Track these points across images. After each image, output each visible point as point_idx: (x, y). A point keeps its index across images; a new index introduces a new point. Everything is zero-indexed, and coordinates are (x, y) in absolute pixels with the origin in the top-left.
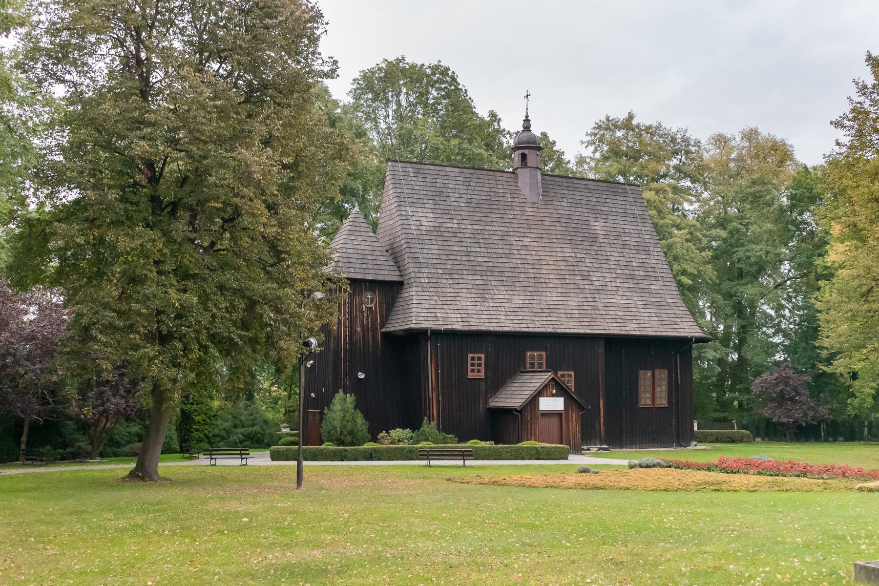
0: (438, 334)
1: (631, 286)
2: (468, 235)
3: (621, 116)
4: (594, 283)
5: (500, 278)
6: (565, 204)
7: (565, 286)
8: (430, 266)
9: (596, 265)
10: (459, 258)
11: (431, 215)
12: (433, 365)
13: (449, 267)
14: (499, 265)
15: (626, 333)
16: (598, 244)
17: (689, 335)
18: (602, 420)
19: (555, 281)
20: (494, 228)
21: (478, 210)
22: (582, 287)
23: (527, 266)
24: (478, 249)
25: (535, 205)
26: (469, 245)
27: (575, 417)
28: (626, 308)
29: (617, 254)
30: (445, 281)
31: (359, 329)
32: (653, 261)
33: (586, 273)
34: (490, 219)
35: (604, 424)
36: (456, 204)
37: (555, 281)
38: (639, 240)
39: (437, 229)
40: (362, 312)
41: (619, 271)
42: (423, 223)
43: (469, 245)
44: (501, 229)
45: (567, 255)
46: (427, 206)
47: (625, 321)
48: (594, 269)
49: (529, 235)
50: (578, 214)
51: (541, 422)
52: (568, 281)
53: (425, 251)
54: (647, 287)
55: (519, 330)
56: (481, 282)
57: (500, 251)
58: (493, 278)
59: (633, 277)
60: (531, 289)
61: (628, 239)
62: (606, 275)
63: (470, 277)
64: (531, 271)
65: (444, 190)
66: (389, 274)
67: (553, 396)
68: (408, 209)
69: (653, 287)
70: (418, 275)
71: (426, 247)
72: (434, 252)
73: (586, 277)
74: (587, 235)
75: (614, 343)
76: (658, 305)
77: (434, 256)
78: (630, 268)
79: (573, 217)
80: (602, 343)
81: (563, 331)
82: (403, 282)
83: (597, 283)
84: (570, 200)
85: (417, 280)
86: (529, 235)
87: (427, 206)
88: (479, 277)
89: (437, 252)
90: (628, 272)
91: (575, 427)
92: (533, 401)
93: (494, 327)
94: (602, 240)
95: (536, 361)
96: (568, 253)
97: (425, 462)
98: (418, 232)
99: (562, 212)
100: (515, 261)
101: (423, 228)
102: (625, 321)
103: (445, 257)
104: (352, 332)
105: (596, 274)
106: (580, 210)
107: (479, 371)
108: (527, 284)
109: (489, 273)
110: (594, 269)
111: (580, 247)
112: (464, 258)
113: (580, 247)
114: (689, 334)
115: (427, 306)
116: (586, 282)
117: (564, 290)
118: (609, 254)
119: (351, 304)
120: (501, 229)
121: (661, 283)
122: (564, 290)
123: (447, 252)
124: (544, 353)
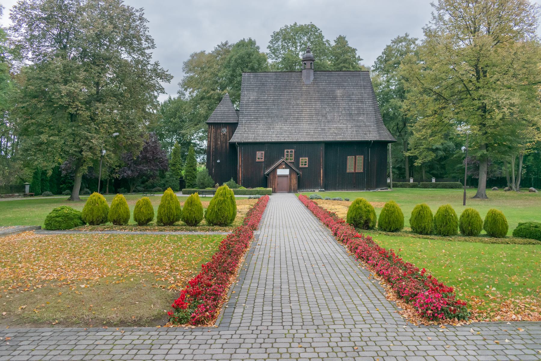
0: (239, 144)
1: (348, 118)
2: (270, 101)
3: (402, 35)
4: (328, 118)
5: (280, 119)
6: (324, 84)
7: (312, 120)
8: (249, 115)
9: (331, 110)
10: (263, 111)
11: (256, 94)
13: (257, 115)
14: (282, 113)
15: (335, 140)
16: (336, 100)
17: (369, 140)
19: (307, 118)
20: (284, 97)
21: (279, 90)
22: (321, 120)
23: (295, 113)
24: (273, 107)
25: (308, 85)
26: (270, 105)
27: (294, 177)
28: (341, 129)
29: (345, 104)
30: (254, 121)
32: (364, 106)
33: (325, 114)
34: (283, 93)
35: (322, 180)
36: (269, 88)
37: (307, 118)
38: (360, 97)
41: (343, 112)
42: (251, 98)
43: (270, 105)
44: (288, 97)
45: (317, 106)
46: (255, 90)
47: (337, 134)
48: (329, 112)
49: (300, 99)
50: (330, 87)
51: (277, 180)
52: (314, 118)
53: (248, 109)
54: (357, 118)
55: (279, 141)
56: (270, 121)
57: (284, 107)
58: (276, 119)
59: (350, 114)
60: (294, 123)
61: (354, 97)
62: (336, 114)
63: (266, 119)
64: (296, 115)
65: (265, 83)
66: (232, 121)
67: (283, 168)
68: (246, 92)
69: (360, 118)
70: (242, 120)
71: (249, 108)
72: (252, 109)
73: (324, 116)
74: (331, 97)
75: (329, 145)
76: (360, 127)
77: (252, 111)
78: (350, 110)
79: (327, 89)
80: (323, 145)
81: (301, 140)
83: (329, 118)
84: (327, 82)
85: (241, 122)
86: (300, 99)
87: (255, 90)
88: (270, 119)
89: (254, 109)
90: (348, 112)
91: (294, 181)
92: (274, 170)
93: (269, 140)
94: (338, 99)
95: (289, 154)
96: (319, 105)
97: (248, 196)
98: (247, 102)
99: (321, 87)
100: (290, 111)
101: (250, 100)
102: (337, 134)
103: (256, 111)
105: (330, 114)
106: (331, 85)
108: (293, 121)
109: (275, 117)
110: (329, 112)
111: (326, 102)
112: (266, 111)
113: (326, 102)
114: (389, 139)
115: (240, 132)
116: (323, 118)
117: (310, 122)
118: (340, 104)
120: (288, 97)
121: (365, 116)
122: (310, 122)
123: (258, 109)
124: (293, 150)
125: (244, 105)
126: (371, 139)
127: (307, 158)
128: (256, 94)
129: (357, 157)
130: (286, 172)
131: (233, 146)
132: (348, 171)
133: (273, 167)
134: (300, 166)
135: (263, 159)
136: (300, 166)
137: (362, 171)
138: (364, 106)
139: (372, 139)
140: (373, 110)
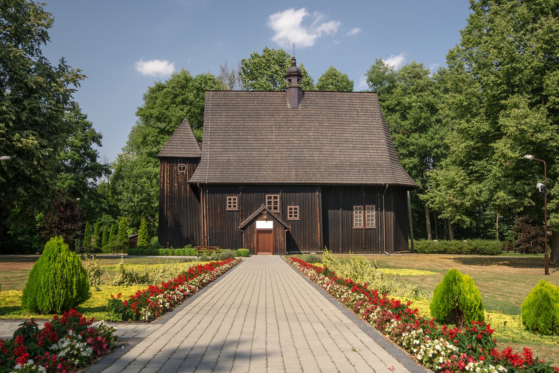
0: (202, 185)
12: (204, 203)
18: (319, 236)
31: (176, 184)
32: (373, 138)
39: (226, 127)
40: (177, 175)
77: (219, 142)
82: (200, 158)
90: (352, 146)
91: (282, 239)
92: (252, 222)
95: (272, 200)
104: (172, 186)
107: (235, 206)
119: (171, 170)
125: (209, 134)
126: (385, 182)
127: (298, 207)
128: (225, 119)
129: (366, 206)
130: (268, 225)
131: (194, 187)
132: (354, 227)
133: (250, 218)
134: (289, 218)
135: (237, 207)
136: (289, 218)
137: (374, 226)
138: (373, 138)
139: (387, 182)
140: (386, 144)
